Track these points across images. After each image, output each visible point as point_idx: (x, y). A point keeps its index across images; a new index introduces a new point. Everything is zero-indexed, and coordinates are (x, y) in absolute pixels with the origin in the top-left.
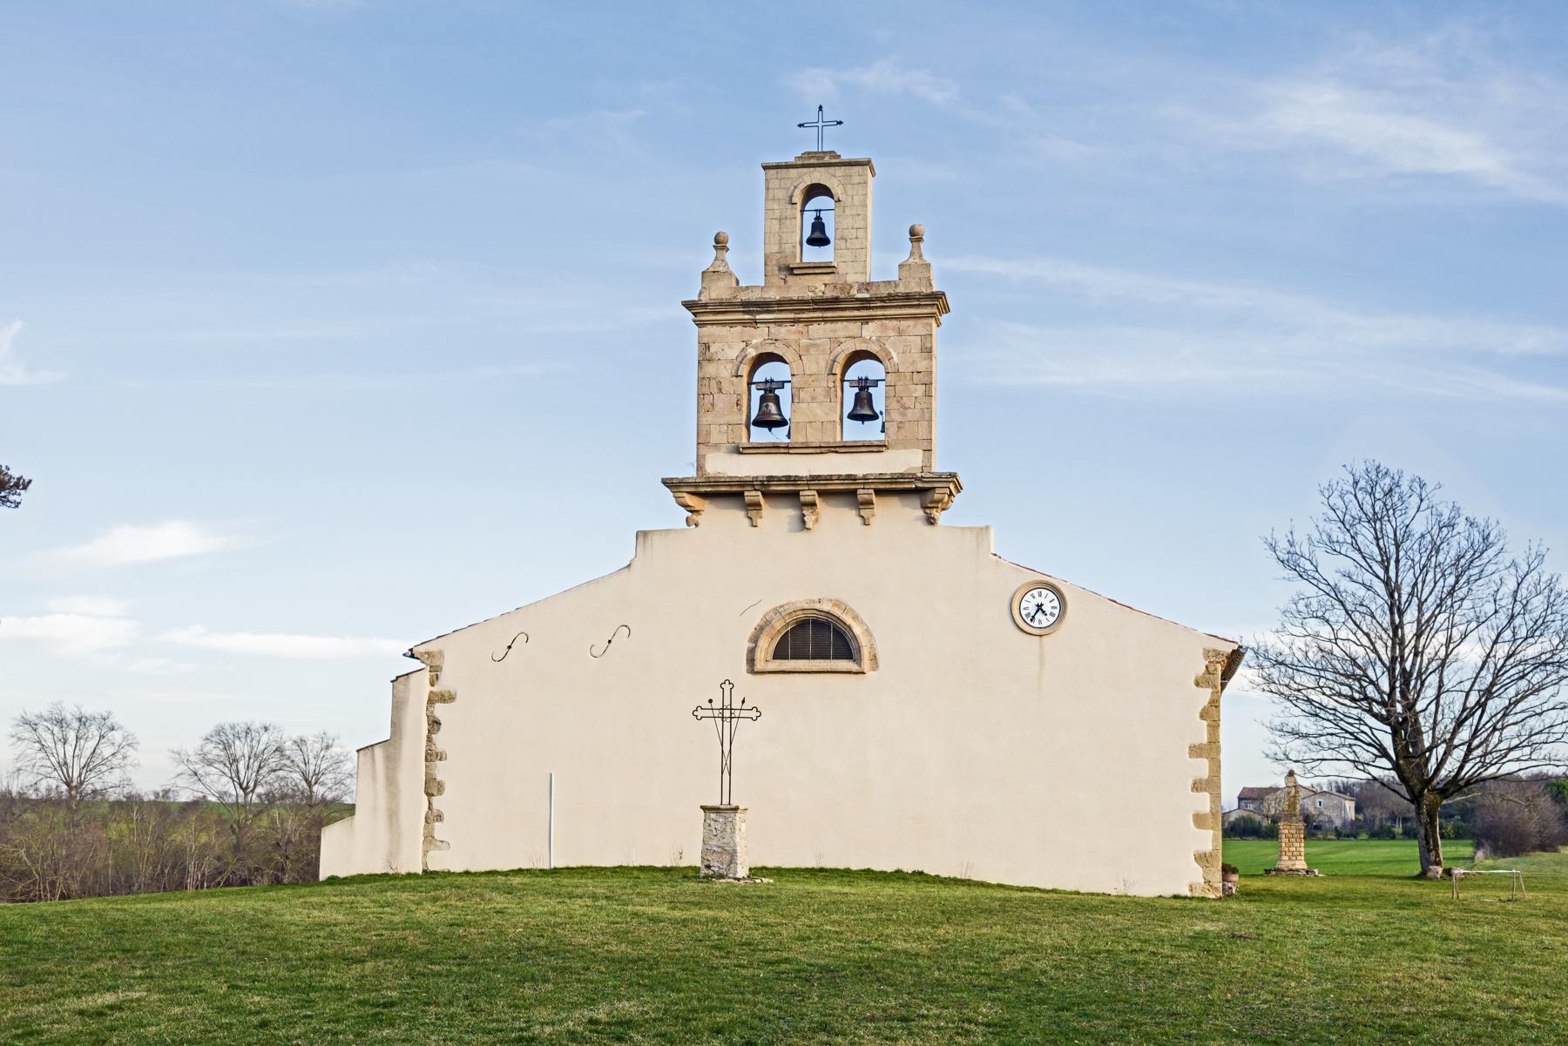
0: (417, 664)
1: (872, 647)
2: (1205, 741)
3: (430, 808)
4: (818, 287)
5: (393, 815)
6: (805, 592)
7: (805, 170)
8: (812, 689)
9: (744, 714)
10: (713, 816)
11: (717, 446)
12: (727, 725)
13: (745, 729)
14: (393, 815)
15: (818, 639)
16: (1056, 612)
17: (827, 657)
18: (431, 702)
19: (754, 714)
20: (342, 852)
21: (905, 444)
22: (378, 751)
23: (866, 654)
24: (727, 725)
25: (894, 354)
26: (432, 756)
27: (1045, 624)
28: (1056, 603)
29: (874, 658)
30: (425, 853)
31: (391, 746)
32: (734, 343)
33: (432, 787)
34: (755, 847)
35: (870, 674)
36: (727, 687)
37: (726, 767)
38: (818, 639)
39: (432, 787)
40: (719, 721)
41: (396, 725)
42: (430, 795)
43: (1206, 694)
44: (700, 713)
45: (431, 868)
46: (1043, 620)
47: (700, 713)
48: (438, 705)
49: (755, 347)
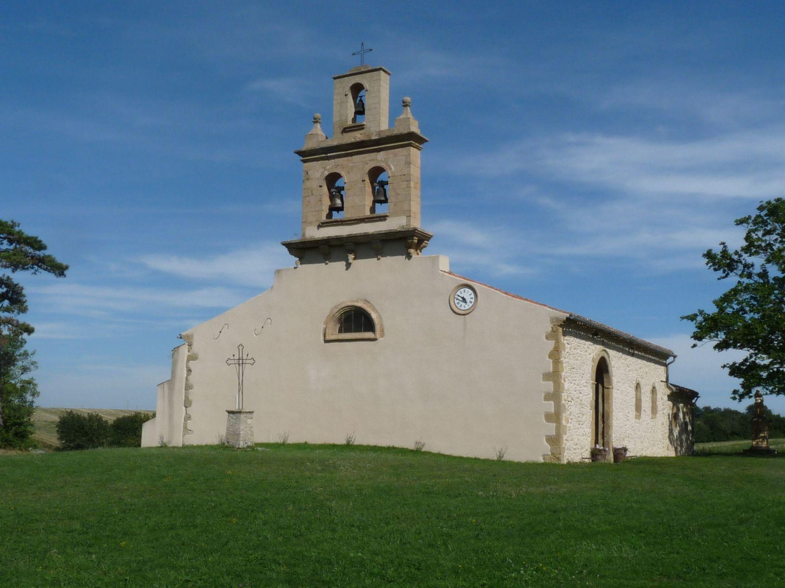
0: (182, 341)
1: (382, 325)
2: (551, 370)
3: (186, 414)
4: (357, 136)
5: (171, 417)
6: (348, 298)
7: (352, 77)
8: (354, 351)
9: (248, 361)
10: (231, 415)
11: (311, 223)
12: (241, 367)
13: (247, 368)
14: (171, 417)
15: (356, 321)
16: (473, 300)
17: (360, 331)
18: (188, 361)
19: (252, 361)
20: (150, 436)
21: (397, 214)
22: (166, 386)
23: (377, 328)
24: (241, 367)
25: (392, 167)
26: (188, 387)
27: (467, 307)
28: (473, 296)
29: (382, 331)
30: (184, 435)
31: (171, 382)
32: (319, 170)
33: (187, 403)
34: (261, 431)
35: (380, 339)
36: (241, 348)
37: (241, 390)
38: (356, 321)
39: (187, 403)
40: (237, 365)
41: (173, 373)
42: (186, 407)
43: (551, 344)
44: (229, 362)
45: (186, 444)
46: (465, 307)
47: (229, 362)
48: (191, 362)
49: (328, 170)
